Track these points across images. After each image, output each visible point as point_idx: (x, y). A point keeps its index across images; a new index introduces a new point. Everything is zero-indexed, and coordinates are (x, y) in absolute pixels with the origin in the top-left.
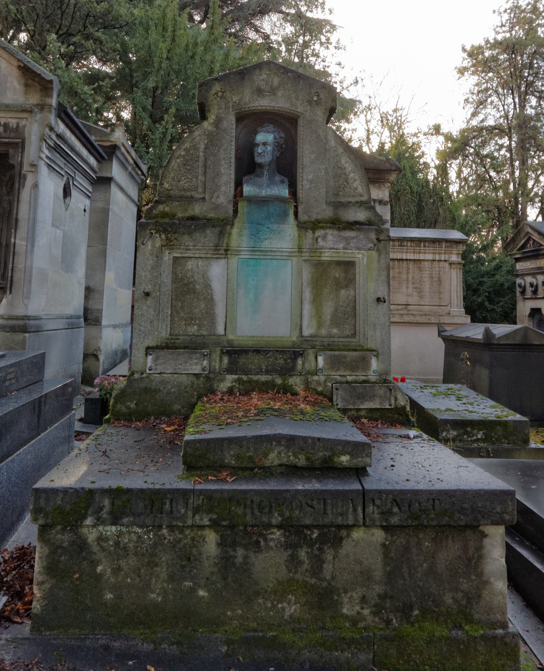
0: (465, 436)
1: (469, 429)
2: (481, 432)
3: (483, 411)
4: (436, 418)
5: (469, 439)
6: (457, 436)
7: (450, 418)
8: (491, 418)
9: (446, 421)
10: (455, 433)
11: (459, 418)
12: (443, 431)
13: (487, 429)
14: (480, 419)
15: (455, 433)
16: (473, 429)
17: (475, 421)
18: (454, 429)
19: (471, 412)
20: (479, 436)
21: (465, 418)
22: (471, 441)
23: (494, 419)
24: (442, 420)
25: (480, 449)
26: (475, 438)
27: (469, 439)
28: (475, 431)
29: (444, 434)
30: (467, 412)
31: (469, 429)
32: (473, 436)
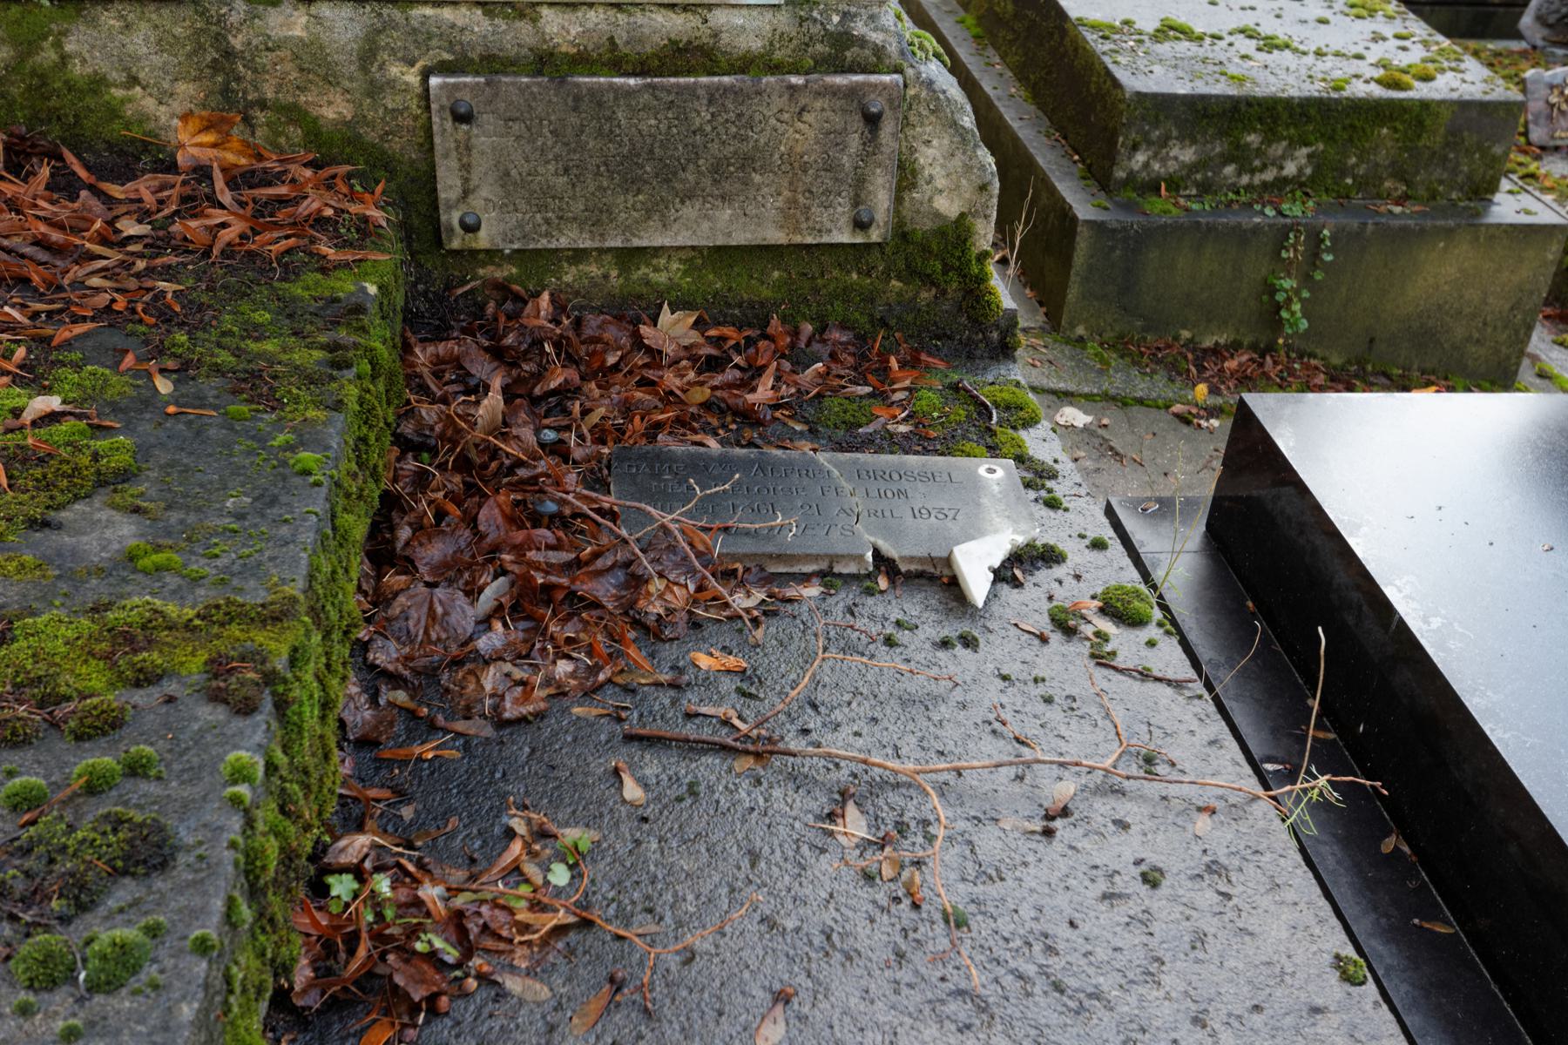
0: (1229, 170)
1: (1253, 139)
2: (1305, 151)
3: (1317, 38)
4: (1116, 84)
5: (1245, 179)
6: (1193, 168)
7: (1182, 89)
8: (1359, 90)
9: (1162, 105)
10: (1187, 155)
11: (1221, 88)
12: (1135, 148)
13: (1330, 139)
14: (1314, 90)
15: (1187, 155)
16: (1271, 136)
17: (1288, 103)
18: (1187, 137)
19: (1270, 44)
20: (1290, 169)
21: (1248, 89)
22: (1249, 188)
23: (1377, 91)
24: (1141, 96)
25: (1284, 232)
26: (1269, 175)
27: (1245, 179)
28: (1278, 149)
29: (1140, 158)
30: (1248, 46)
31: (1253, 139)
32: (1264, 167)
